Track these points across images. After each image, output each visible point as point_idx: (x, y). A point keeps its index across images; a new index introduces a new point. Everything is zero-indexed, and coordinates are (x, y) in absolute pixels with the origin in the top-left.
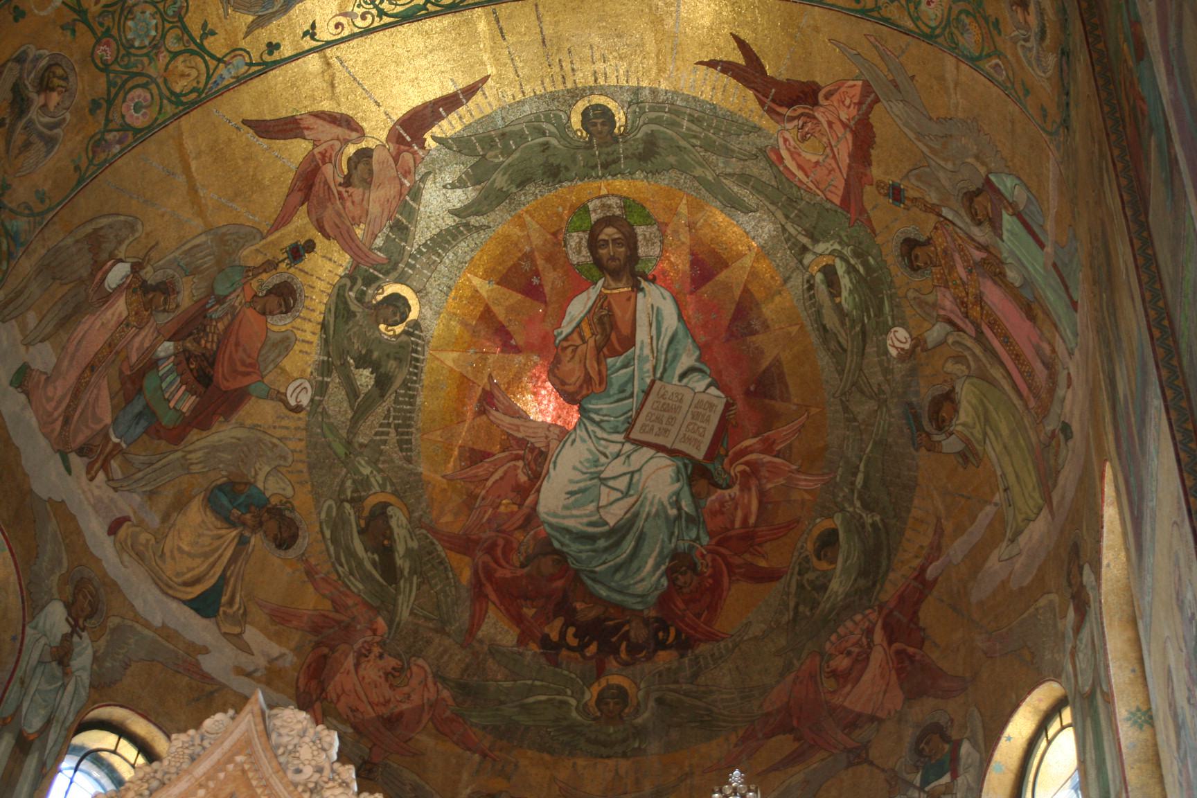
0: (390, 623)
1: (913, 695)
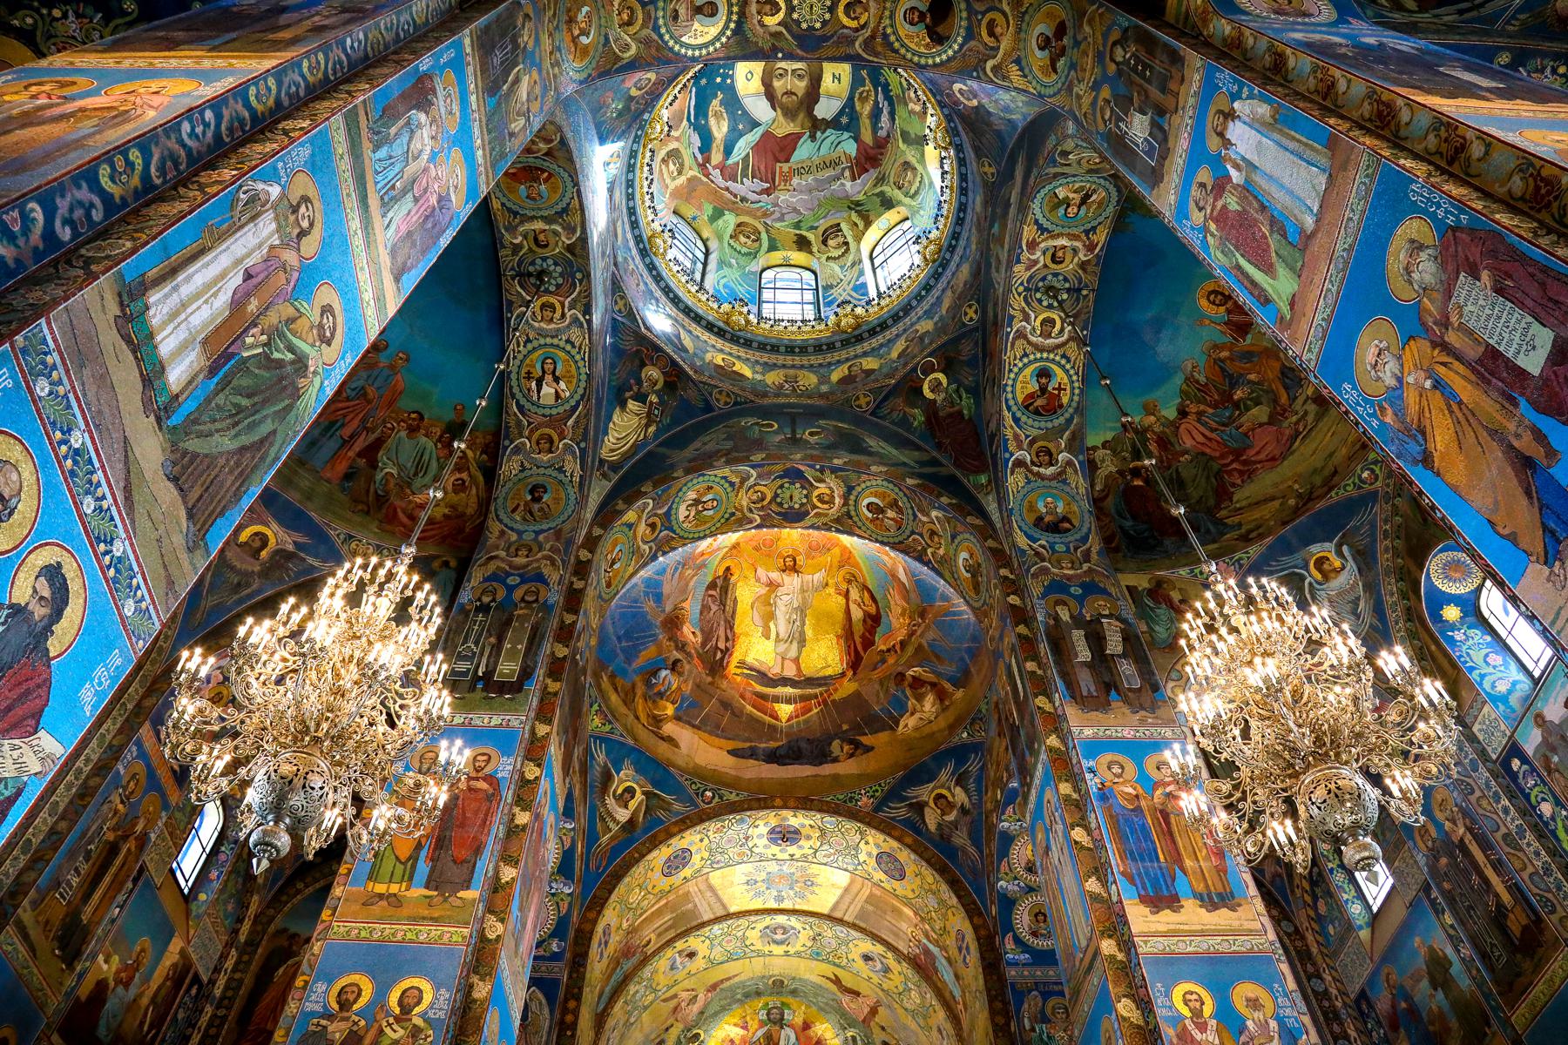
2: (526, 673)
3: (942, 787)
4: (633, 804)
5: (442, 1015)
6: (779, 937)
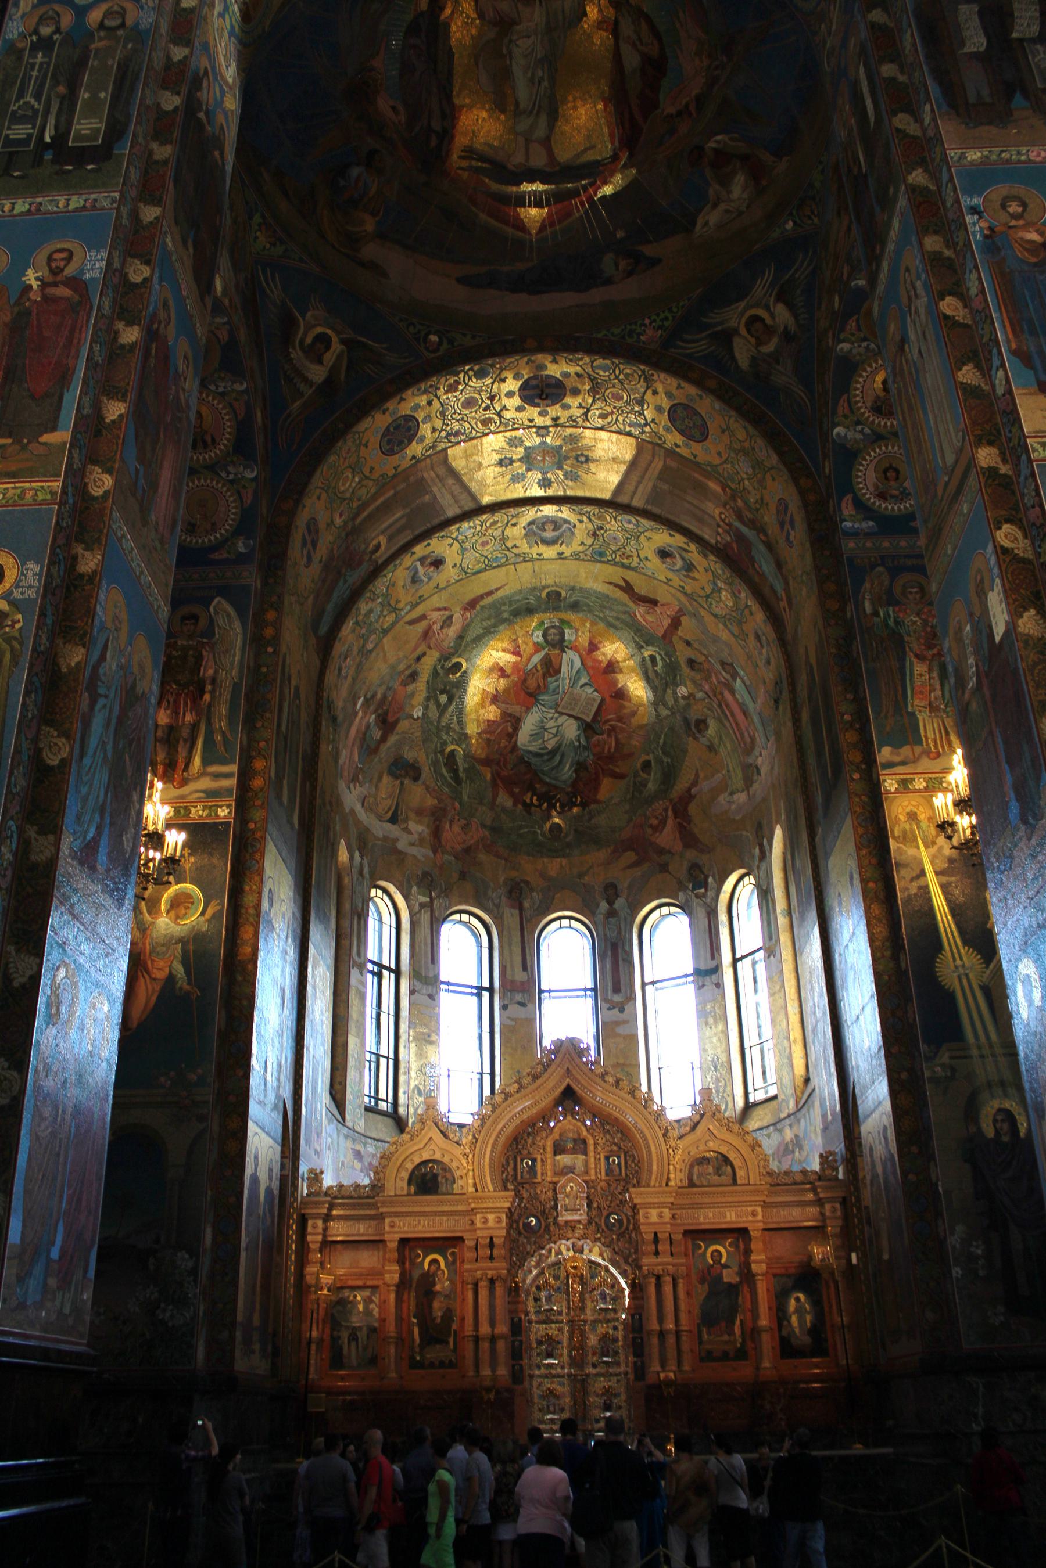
0: (460, 804)
1: (687, 846)
2: (115, 131)
3: (757, 305)
4: (329, 358)
5: (33, 595)
6: (549, 534)
